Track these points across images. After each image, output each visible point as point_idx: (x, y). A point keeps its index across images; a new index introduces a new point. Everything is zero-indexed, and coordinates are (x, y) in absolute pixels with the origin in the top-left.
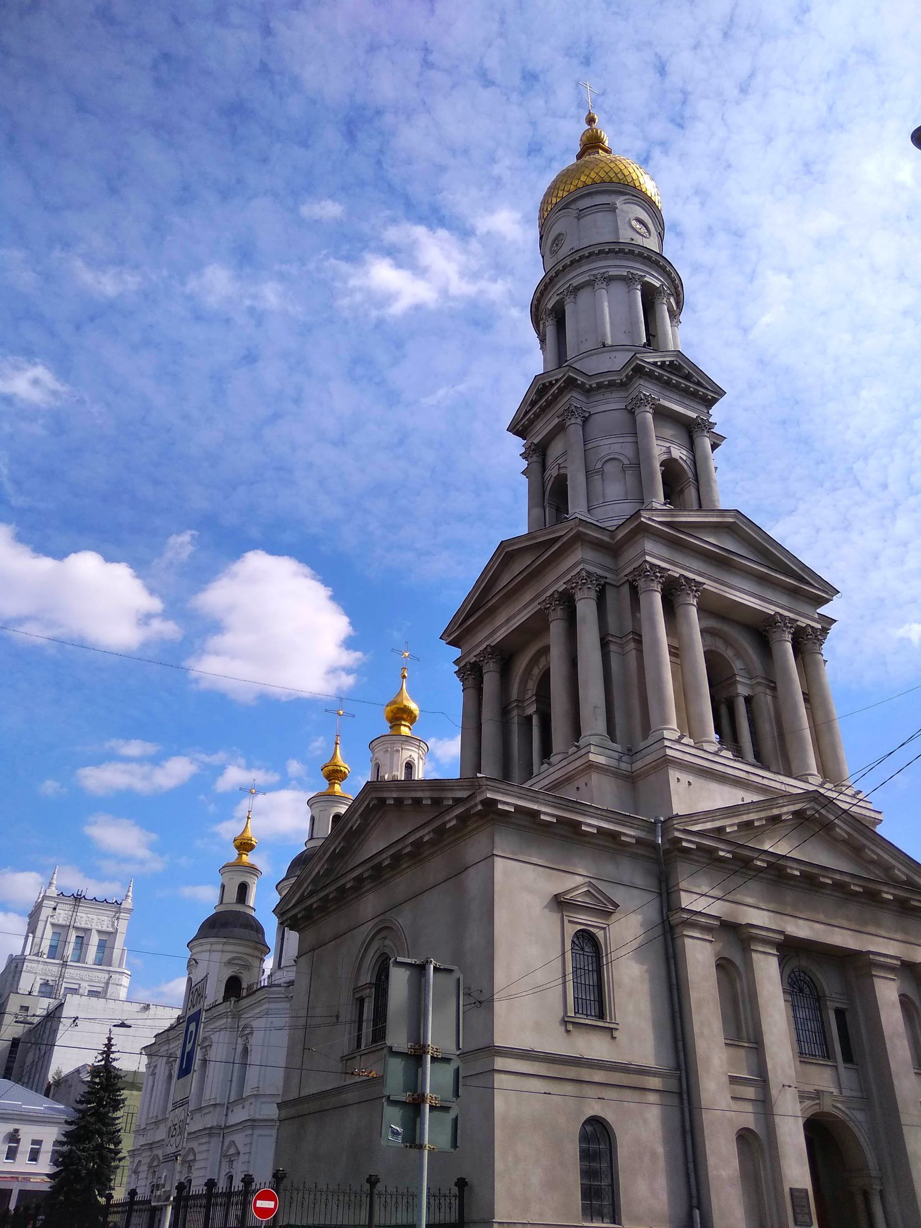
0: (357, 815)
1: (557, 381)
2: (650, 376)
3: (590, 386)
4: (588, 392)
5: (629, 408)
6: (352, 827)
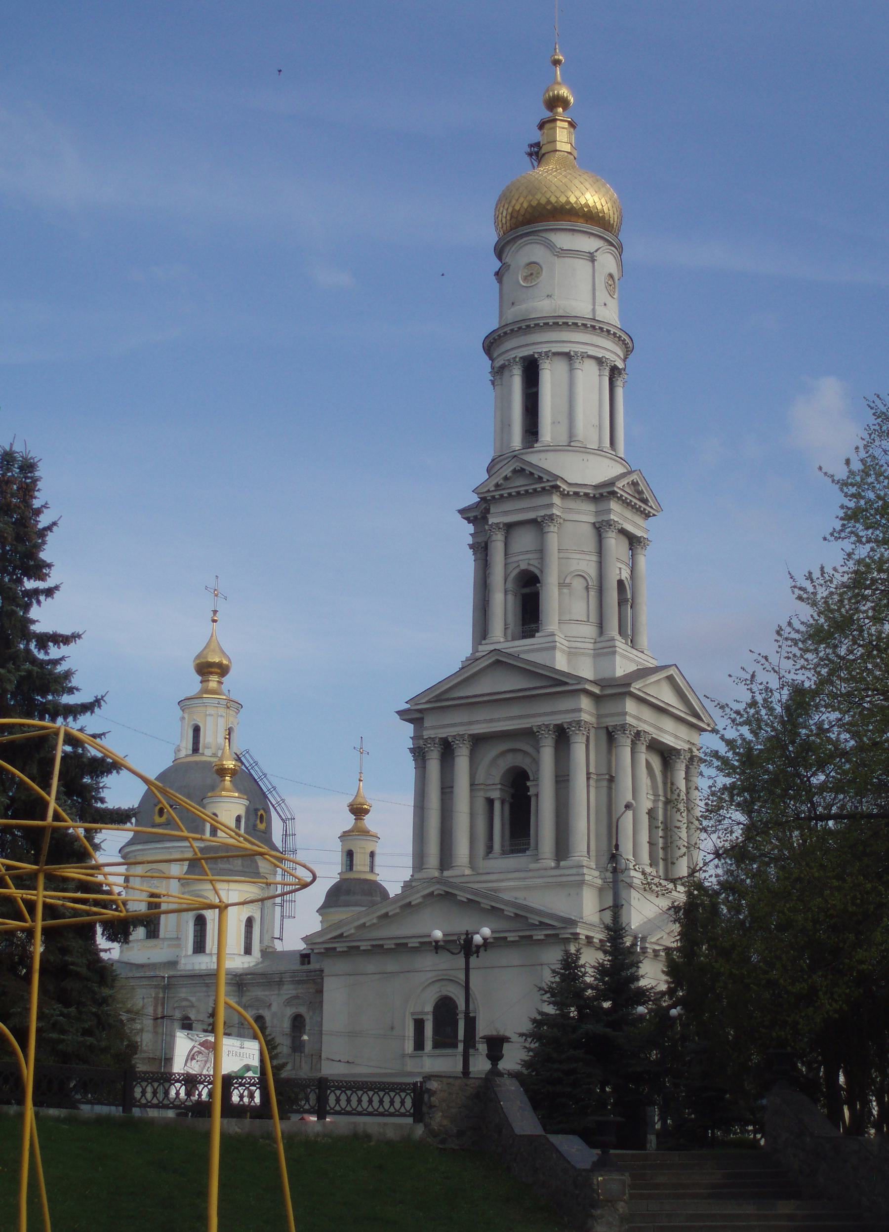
0: (418, 895)
1: (540, 478)
2: (620, 498)
3: (568, 492)
4: (565, 495)
5: (597, 526)
6: (410, 902)
